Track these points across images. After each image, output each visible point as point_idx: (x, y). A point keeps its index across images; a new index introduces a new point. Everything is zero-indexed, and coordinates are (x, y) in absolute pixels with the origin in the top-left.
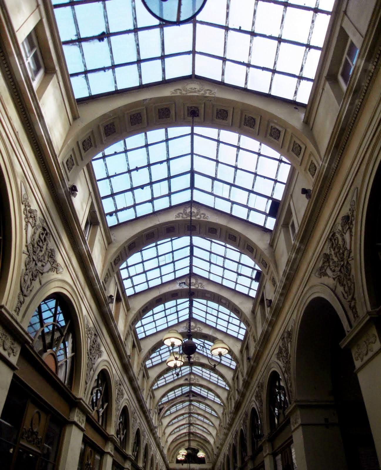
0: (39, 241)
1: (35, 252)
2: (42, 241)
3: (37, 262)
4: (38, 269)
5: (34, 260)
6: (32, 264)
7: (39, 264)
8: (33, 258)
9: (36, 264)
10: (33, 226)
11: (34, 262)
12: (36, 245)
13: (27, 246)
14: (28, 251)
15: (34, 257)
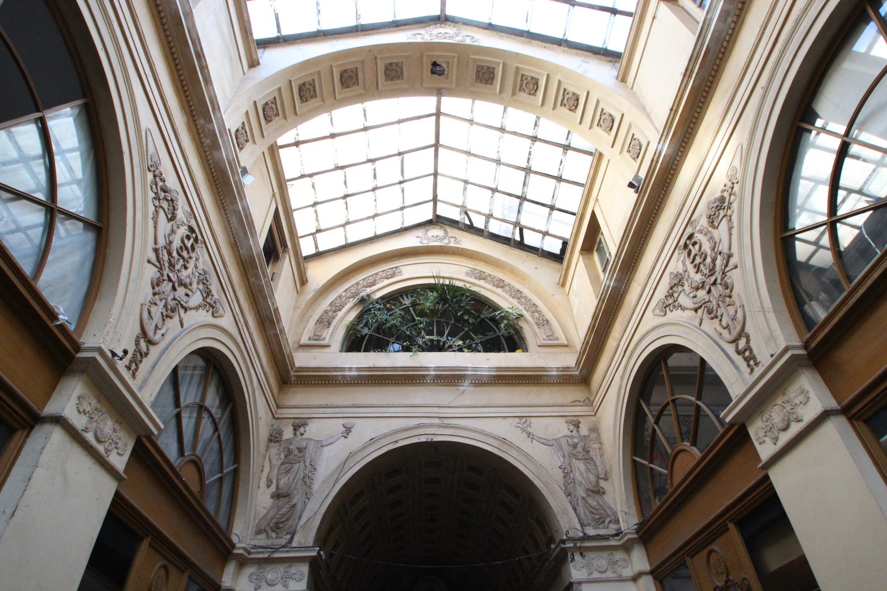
0: (181, 248)
1: (174, 267)
2: (187, 249)
3: (176, 285)
4: (177, 297)
5: (170, 280)
6: (166, 287)
7: (181, 291)
8: (168, 276)
9: (174, 289)
10: (169, 216)
11: (171, 284)
12: (175, 254)
13: (156, 251)
14: (158, 260)
15: (171, 275)
